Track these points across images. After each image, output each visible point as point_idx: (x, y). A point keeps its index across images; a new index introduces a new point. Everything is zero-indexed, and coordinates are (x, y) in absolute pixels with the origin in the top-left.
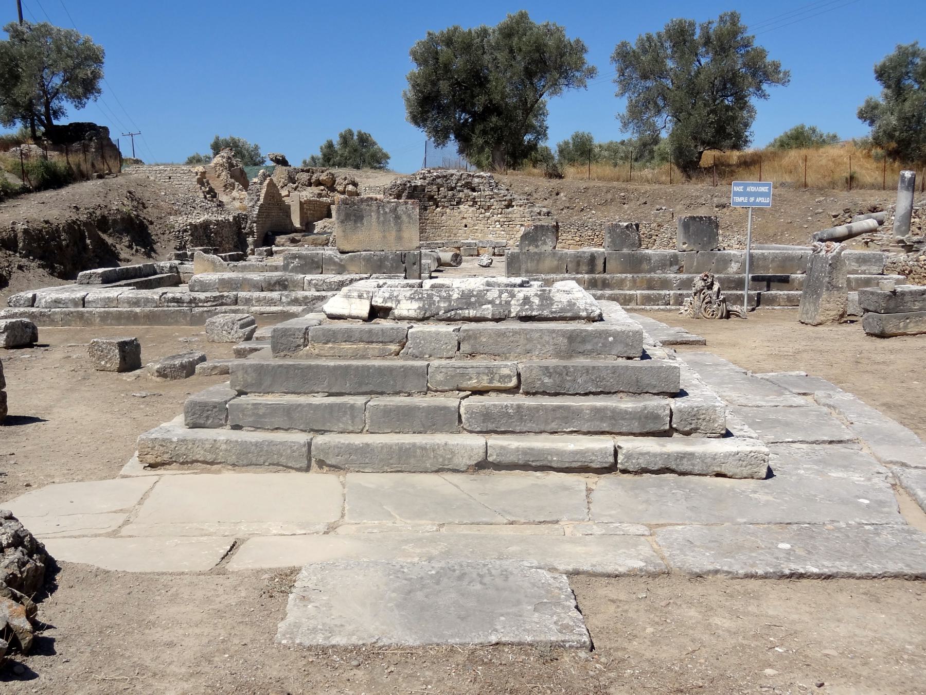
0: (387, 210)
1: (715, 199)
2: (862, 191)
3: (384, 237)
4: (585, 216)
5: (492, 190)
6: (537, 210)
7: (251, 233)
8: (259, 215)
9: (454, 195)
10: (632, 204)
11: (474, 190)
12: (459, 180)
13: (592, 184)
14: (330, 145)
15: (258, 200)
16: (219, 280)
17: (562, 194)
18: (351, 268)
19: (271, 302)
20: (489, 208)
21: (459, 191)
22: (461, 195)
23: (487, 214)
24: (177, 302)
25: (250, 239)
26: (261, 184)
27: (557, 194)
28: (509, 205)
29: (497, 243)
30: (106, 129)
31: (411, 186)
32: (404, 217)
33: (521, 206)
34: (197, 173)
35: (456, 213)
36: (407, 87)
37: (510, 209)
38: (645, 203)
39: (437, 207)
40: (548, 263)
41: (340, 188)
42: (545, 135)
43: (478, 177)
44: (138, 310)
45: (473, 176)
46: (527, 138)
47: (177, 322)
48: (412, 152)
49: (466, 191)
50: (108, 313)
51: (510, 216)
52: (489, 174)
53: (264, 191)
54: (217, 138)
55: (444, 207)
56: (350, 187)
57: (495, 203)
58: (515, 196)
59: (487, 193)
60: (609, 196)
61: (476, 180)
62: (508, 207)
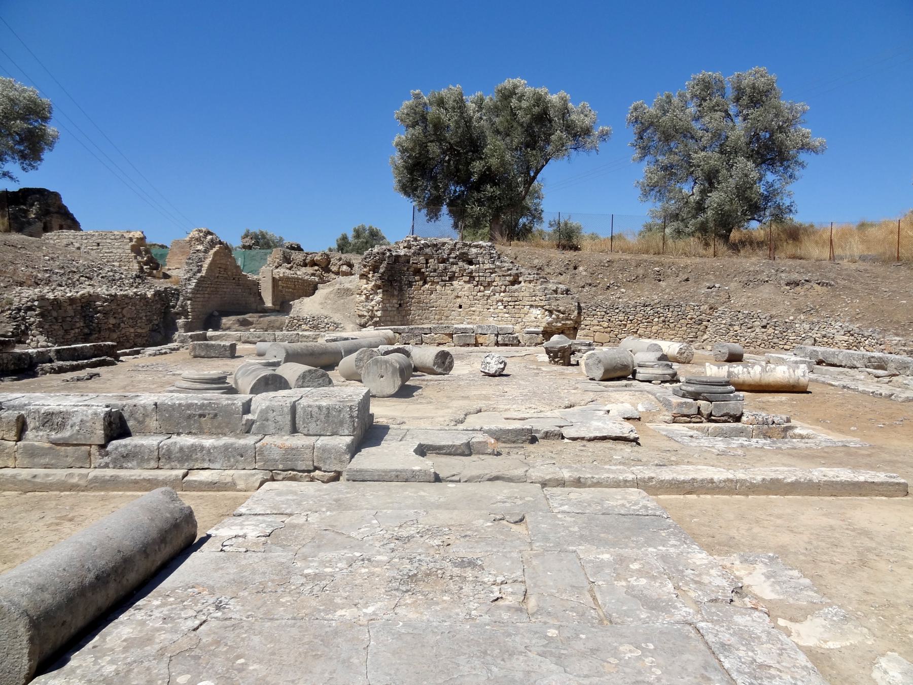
1: (783, 275)
4: (613, 295)
5: (493, 263)
6: (552, 286)
7: (184, 313)
8: (195, 291)
9: (446, 269)
10: (671, 280)
11: (470, 263)
12: (452, 250)
13: (616, 257)
14: (344, 238)
15: (199, 271)
17: (581, 268)
20: (489, 284)
21: (453, 264)
22: (455, 268)
23: (487, 292)
25: (181, 321)
26: (206, 251)
27: (575, 268)
28: (515, 282)
29: (501, 329)
30: (56, 195)
31: (391, 255)
33: (530, 282)
34: (131, 239)
35: (448, 290)
36: (397, 156)
37: (516, 286)
38: (687, 280)
39: (425, 283)
41: (334, 269)
42: (540, 218)
43: (476, 246)
45: (470, 246)
46: (523, 221)
48: (402, 225)
49: (461, 264)
51: (516, 294)
52: (489, 244)
53: (208, 261)
54: (248, 231)
55: (433, 283)
56: (345, 268)
57: (497, 279)
58: (523, 270)
59: (487, 266)
60: (640, 271)
61: (474, 250)
62: (513, 283)
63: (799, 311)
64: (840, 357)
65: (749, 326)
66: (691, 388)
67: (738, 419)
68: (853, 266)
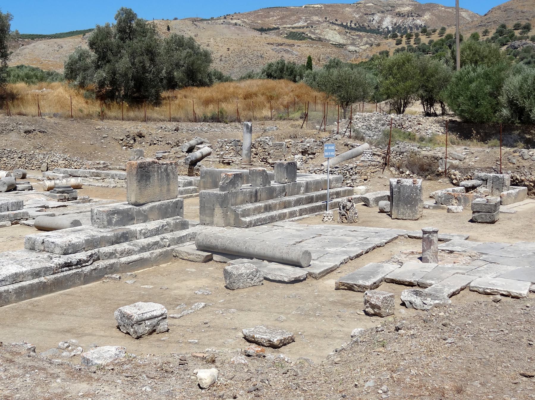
0: (163, 170)
2: (110, 121)
3: (161, 190)
16: (86, 240)
18: (151, 217)
19: (129, 253)
24: (68, 266)
32: (171, 175)
40: (240, 198)
44: (42, 279)
47: (74, 285)
50: (22, 288)
63: (35, 148)
64: (79, 173)
65: (12, 157)
66: (60, 190)
67: (76, 199)
68: (52, 120)
